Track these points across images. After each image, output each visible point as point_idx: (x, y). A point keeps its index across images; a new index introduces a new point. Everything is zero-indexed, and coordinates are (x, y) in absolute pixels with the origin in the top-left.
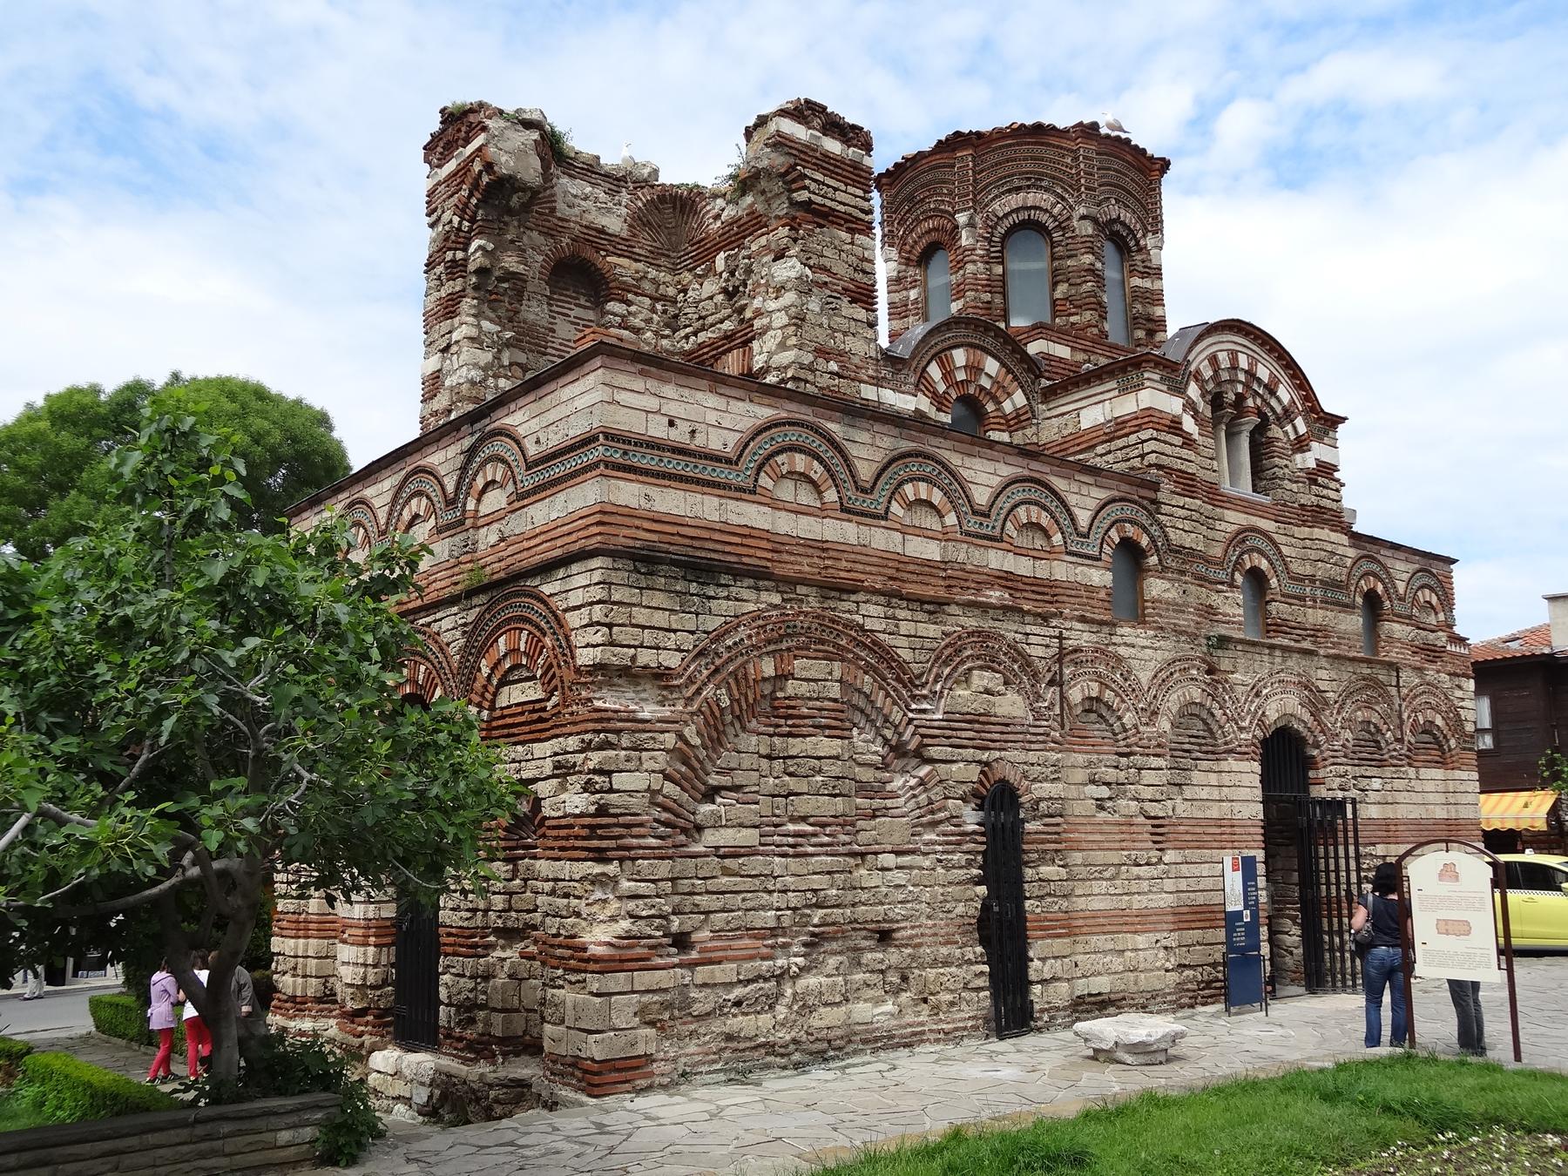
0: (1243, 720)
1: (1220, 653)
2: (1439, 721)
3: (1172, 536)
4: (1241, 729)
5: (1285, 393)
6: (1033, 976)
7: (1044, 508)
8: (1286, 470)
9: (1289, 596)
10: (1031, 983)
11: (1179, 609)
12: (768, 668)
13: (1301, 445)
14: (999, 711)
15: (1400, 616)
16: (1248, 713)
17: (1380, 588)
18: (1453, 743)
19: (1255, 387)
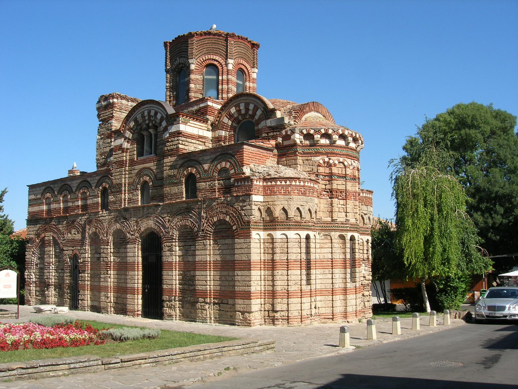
0: (132, 231)
1: (126, 213)
2: (228, 219)
3: (114, 181)
4: (132, 235)
5: (159, 116)
6: (79, 298)
7: (86, 187)
8: (161, 141)
9: (156, 187)
10: (79, 300)
11: (114, 203)
12: (43, 235)
13: (166, 129)
14: (76, 238)
15: (204, 179)
16: (134, 230)
17: (194, 171)
18: (234, 228)
19: (152, 119)
